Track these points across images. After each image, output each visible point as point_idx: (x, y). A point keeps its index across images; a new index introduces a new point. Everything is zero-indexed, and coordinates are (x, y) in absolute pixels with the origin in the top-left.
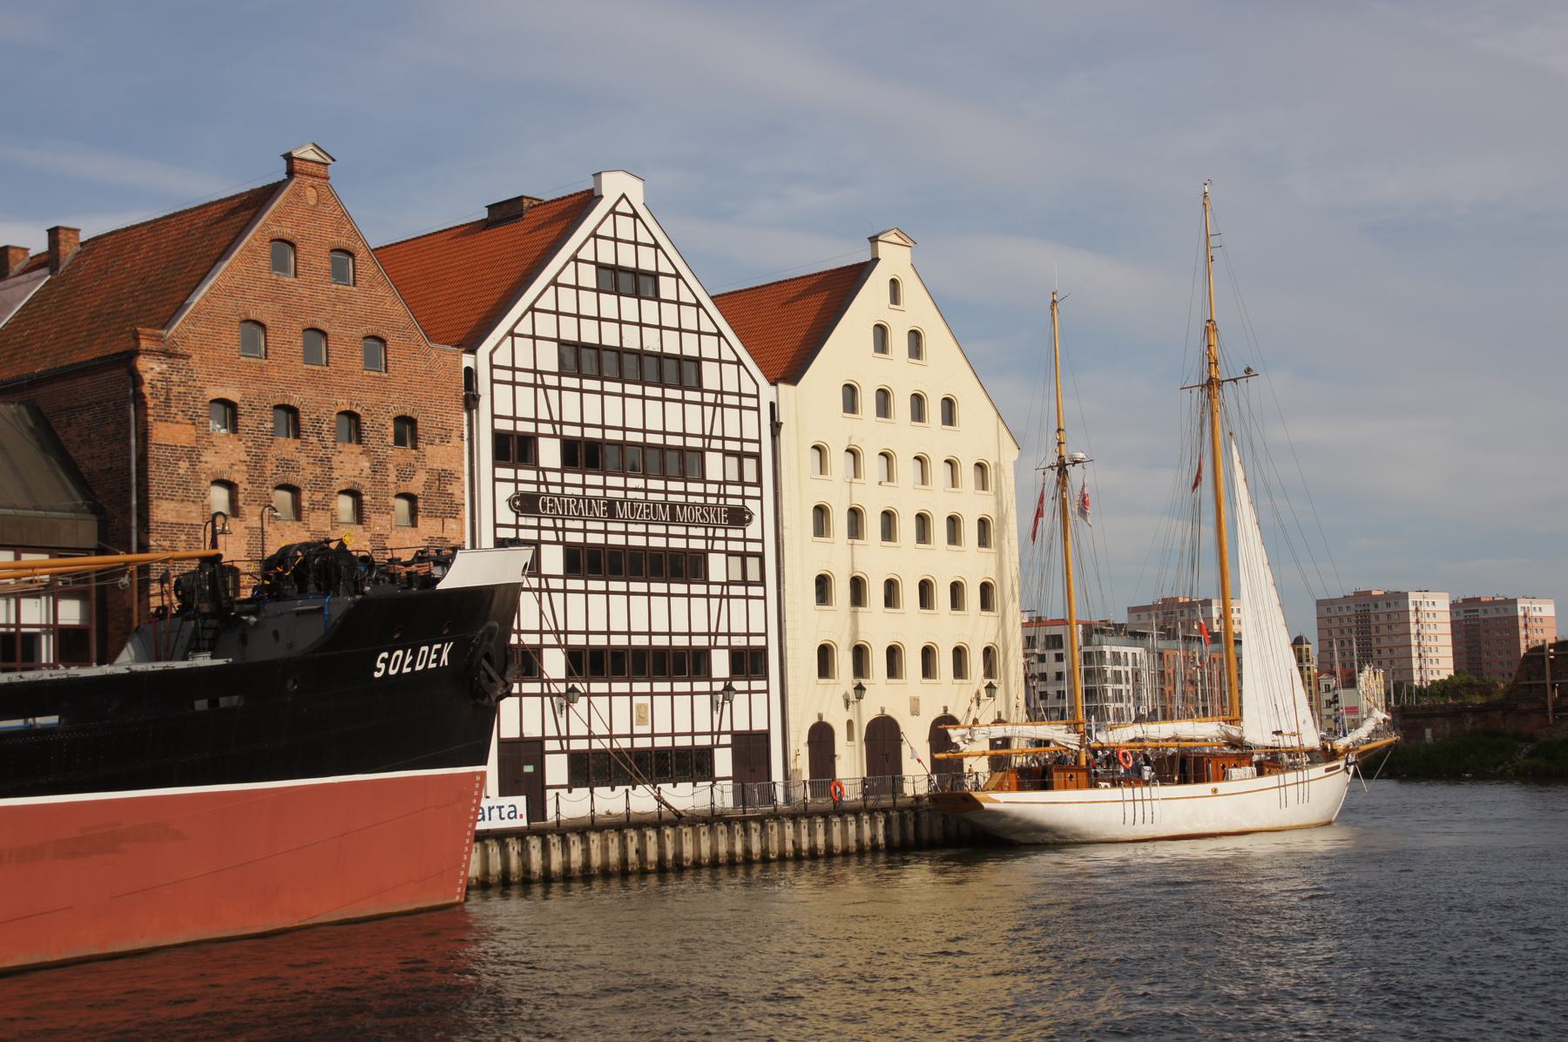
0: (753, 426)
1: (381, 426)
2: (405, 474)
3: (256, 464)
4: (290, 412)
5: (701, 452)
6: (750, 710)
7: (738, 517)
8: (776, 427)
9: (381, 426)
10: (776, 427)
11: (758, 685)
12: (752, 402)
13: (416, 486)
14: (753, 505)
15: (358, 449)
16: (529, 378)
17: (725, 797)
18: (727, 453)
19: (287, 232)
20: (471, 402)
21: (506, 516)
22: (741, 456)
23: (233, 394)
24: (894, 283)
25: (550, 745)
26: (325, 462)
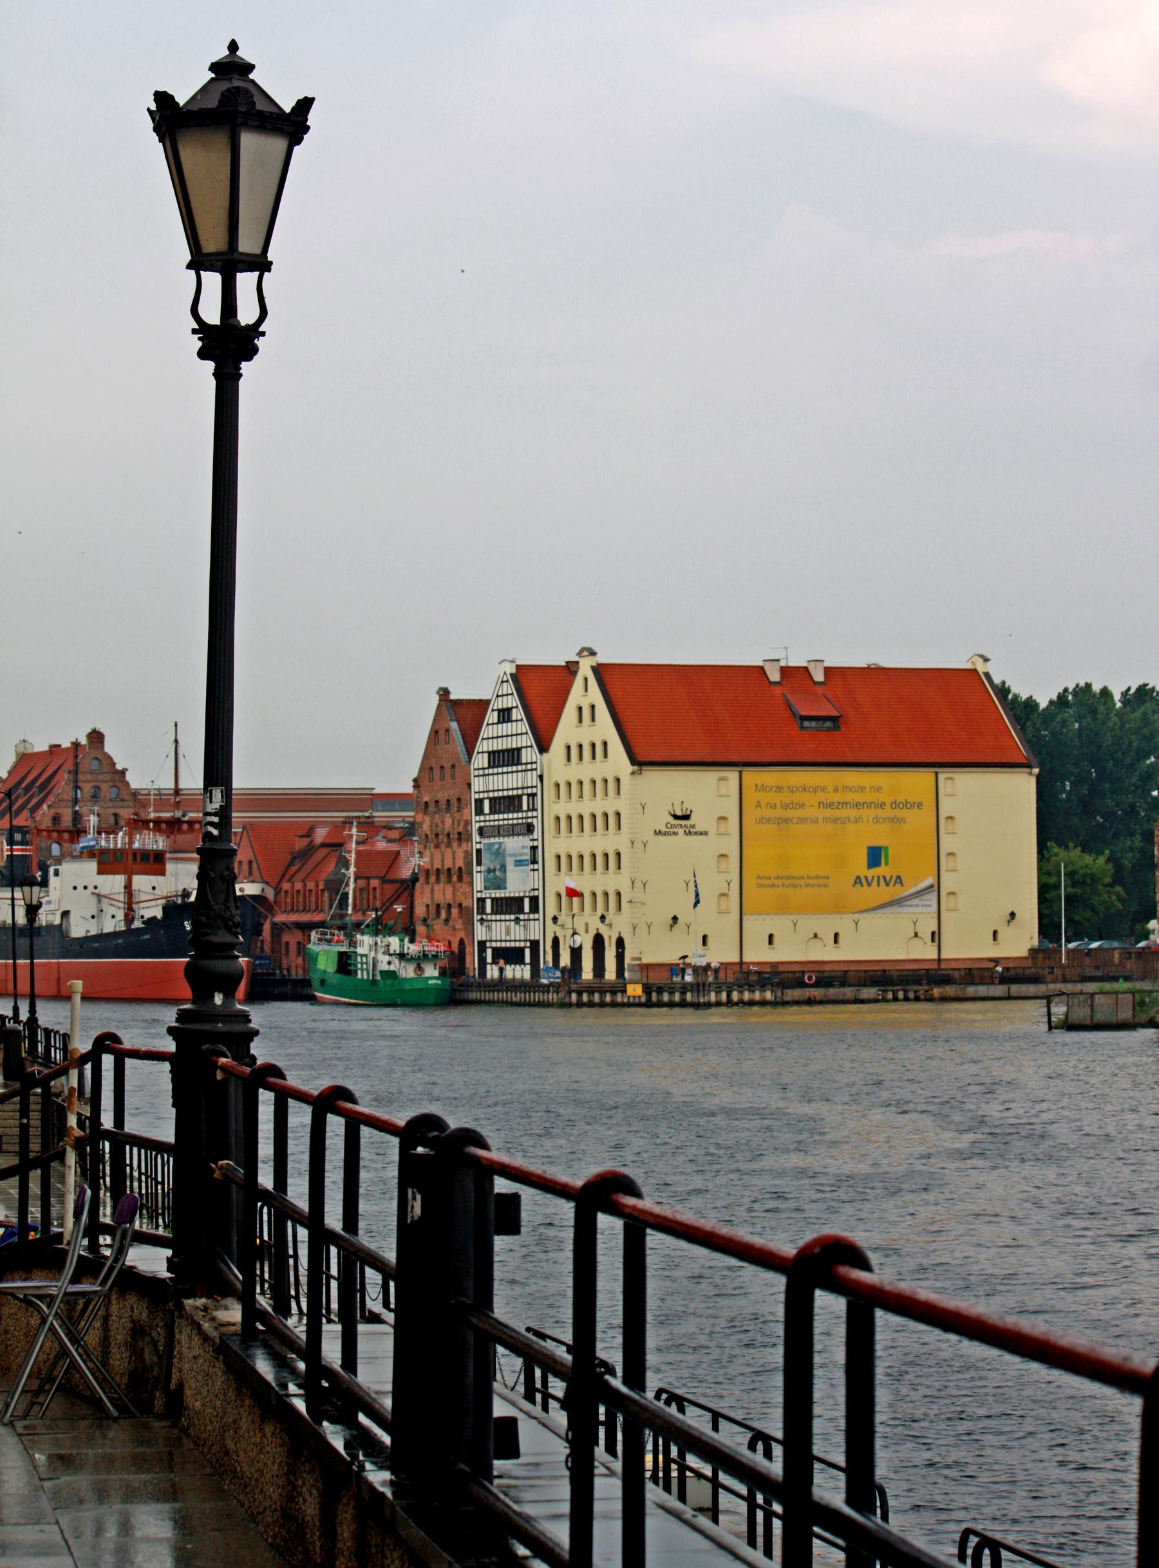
0: (532, 779)
1: (454, 803)
2: (459, 824)
3: (431, 827)
4: (437, 802)
5: (520, 797)
6: (535, 933)
7: (530, 828)
8: (541, 777)
9: (454, 803)
10: (541, 777)
11: (536, 916)
12: (534, 766)
13: (461, 829)
14: (535, 821)
15: (448, 815)
16: (481, 772)
17: (521, 972)
18: (528, 795)
19: (437, 727)
20: (469, 785)
21: (478, 839)
22: (534, 795)
23: (426, 799)
24: (586, 679)
25: (488, 944)
26: (443, 822)
